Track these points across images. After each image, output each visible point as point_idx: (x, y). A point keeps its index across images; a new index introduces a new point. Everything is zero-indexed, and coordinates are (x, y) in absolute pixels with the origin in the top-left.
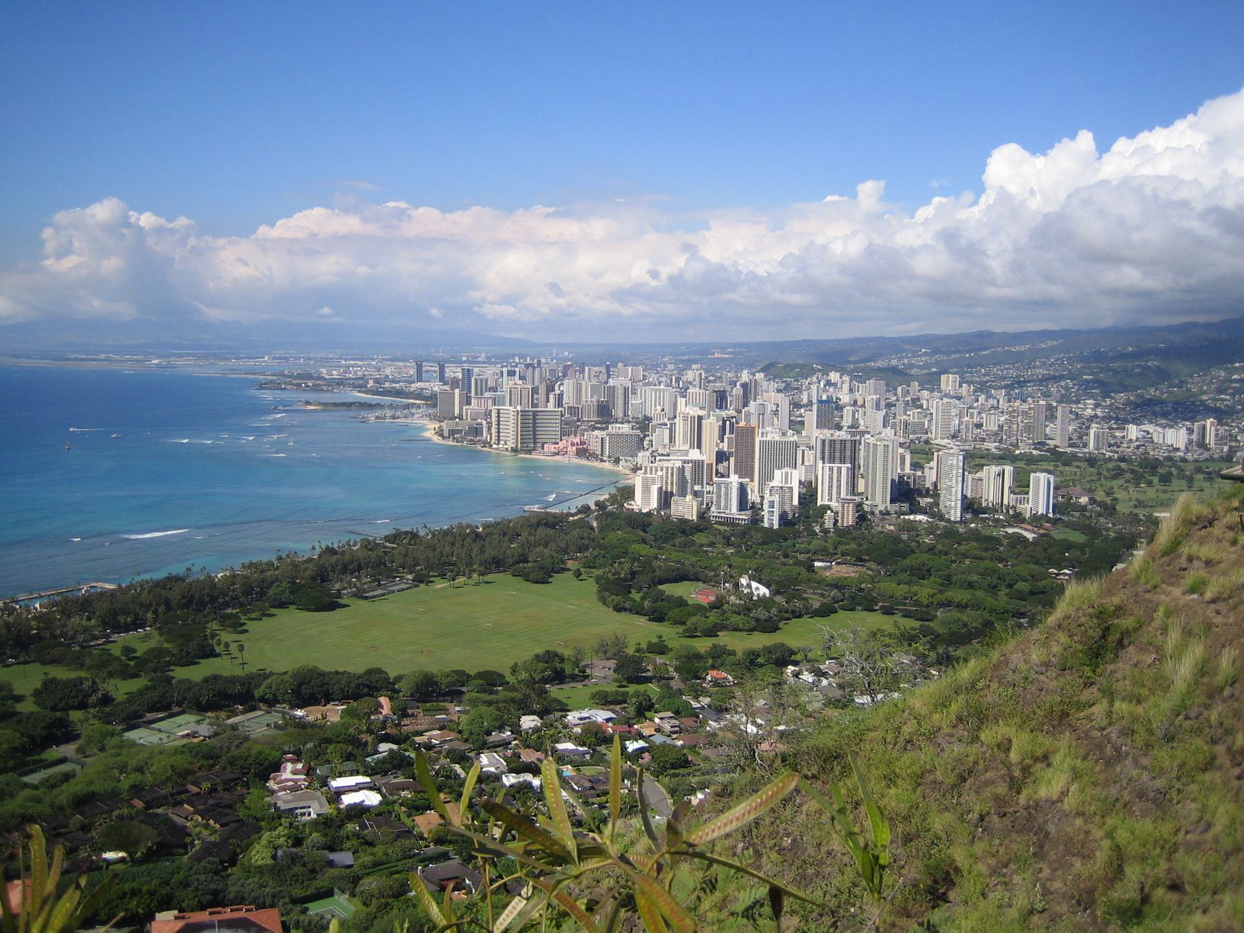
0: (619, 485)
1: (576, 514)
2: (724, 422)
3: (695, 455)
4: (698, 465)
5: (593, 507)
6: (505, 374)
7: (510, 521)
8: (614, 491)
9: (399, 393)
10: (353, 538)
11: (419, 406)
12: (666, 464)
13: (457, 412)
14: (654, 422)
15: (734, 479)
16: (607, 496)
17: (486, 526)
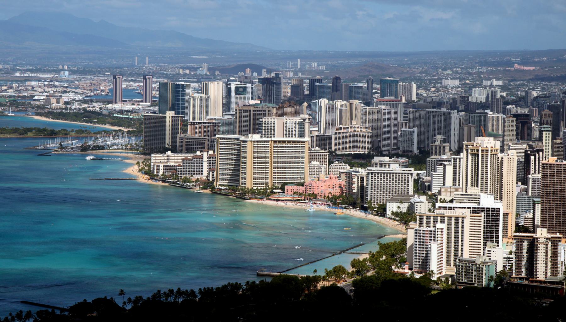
0: (384, 241)
1: (324, 279)
2: (527, 157)
3: (488, 201)
4: (491, 215)
5: (350, 269)
6: (233, 90)
7: (237, 286)
8: (375, 248)
9: (87, 116)
10: (25, 309)
11: (115, 135)
12: (448, 213)
13: (168, 140)
14: (434, 157)
15: (542, 233)
16: (367, 256)
17: (207, 293)
